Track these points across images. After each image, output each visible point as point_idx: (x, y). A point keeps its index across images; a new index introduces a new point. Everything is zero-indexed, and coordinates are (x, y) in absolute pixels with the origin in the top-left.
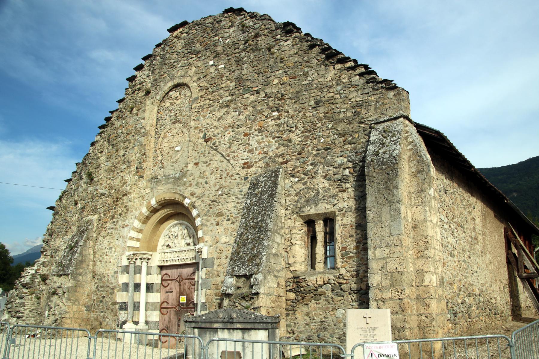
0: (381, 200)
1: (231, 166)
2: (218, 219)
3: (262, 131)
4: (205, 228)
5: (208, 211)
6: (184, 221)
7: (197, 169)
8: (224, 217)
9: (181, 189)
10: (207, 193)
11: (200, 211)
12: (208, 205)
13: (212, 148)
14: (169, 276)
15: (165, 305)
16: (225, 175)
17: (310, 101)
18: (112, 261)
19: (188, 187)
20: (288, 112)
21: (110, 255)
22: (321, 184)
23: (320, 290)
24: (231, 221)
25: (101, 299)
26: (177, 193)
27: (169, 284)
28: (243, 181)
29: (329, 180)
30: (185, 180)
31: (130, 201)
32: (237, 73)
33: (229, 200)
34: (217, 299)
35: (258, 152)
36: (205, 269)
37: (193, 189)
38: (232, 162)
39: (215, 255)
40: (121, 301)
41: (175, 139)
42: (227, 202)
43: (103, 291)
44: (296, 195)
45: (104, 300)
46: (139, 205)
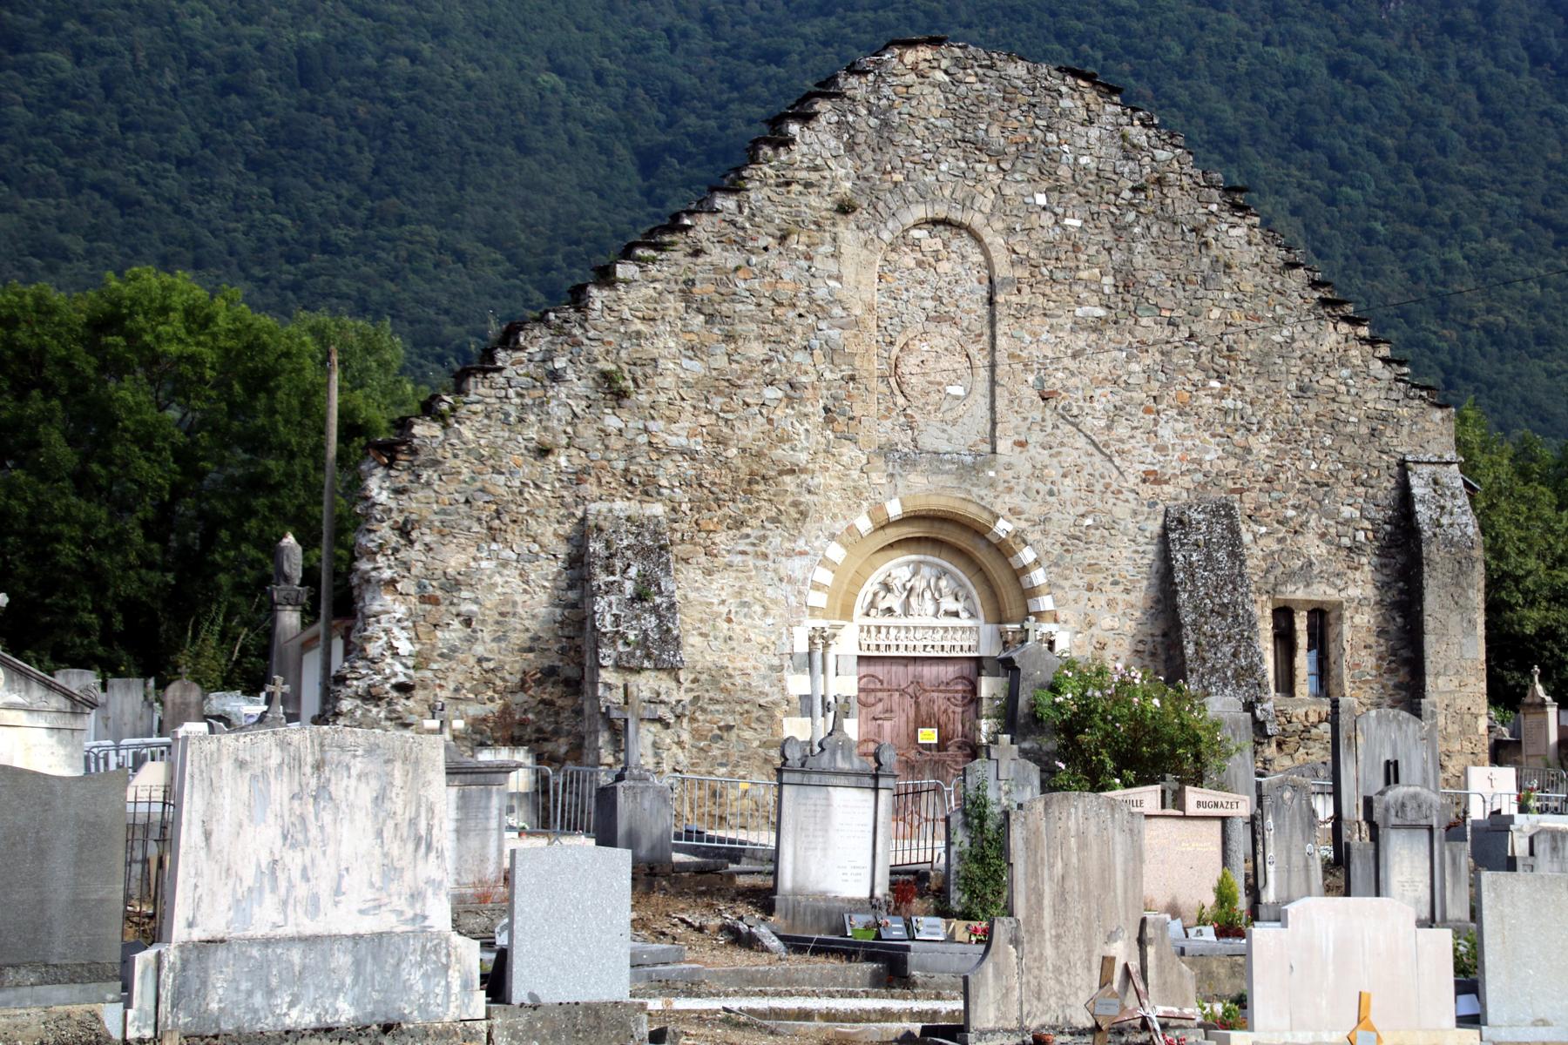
0: (1449, 602)
1: (1116, 473)
2: (1087, 578)
3: (1188, 414)
4: (1059, 593)
5: (1061, 557)
9: (983, 493)
10: (1056, 516)
11: (1042, 553)
14: (881, 682)
16: (1098, 487)
17: (1288, 382)
20: (1242, 389)
21: (748, 621)
22: (1313, 547)
23: (1314, 731)
24: (1121, 587)
28: (1146, 509)
29: (1330, 543)
30: (992, 474)
31: (809, 492)
32: (1117, 256)
35: (1177, 454)
37: (1016, 500)
38: (1117, 460)
41: (945, 363)
43: (724, 712)
44: (1264, 559)
45: (733, 735)
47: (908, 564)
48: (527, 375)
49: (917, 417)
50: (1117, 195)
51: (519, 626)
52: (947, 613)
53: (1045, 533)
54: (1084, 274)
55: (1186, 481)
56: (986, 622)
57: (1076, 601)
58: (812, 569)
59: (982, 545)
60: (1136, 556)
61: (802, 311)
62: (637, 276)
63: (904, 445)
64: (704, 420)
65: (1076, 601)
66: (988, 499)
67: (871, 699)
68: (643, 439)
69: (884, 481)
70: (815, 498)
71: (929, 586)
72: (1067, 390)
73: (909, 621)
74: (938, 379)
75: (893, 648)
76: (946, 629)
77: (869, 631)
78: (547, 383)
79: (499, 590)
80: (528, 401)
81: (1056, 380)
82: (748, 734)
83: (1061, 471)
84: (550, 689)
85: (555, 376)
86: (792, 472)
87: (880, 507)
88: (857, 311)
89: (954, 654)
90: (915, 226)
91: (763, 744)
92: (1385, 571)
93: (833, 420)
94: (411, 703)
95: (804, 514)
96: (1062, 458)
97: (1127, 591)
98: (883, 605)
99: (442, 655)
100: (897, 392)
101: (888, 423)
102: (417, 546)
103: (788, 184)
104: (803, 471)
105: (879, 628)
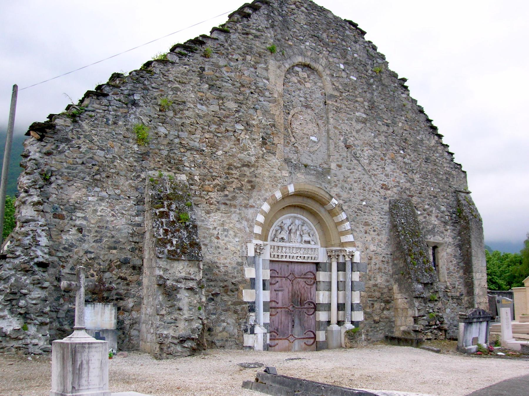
2: (366, 228)
4: (355, 234)
6: (303, 215)
8: (370, 227)
11: (348, 215)
14: (278, 273)
15: (273, 305)
18: (229, 247)
21: (227, 239)
24: (376, 233)
25: (212, 297)
27: (277, 282)
28: (383, 200)
30: (329, 178)
31: (256, 176)
33: (373, 213)
34: (370, 301)
36: (358, 272)
39: (366, 261)
42: (372, 214)
45: (218, 299)
48: (120, 101)
49: (299, 148)
50: (367, 72)
51: (109, 235)
54: (359, 99)
55: (395, 190)
56: (321, 247)
59: (322, 210)
60: (380, 219)
61: (253, 91)
62: (177, 61)
64: (207, 136)
66: (328, 189)
68: (177, 141)
69: (287, 175)
73: (291, 245)
78: (130, 106)
79: (99, 214)
80: (119, 114)
81: (350, 141)
82: (226, 298)
83: (354, 180)
84: (124, 271)
85: (134, 103)
86: (248, 166)
87: (286, 187)
88: (276, 96)
90: (297, 65)
91: (234, 304)
92: (454, 232)
94: (46, 275)
95: (253, 187)
97: (378, 235)
98: (280, 236)
99: (65, 248)
102: (53, 185)
103: (247, 34)
105: (278, 247)
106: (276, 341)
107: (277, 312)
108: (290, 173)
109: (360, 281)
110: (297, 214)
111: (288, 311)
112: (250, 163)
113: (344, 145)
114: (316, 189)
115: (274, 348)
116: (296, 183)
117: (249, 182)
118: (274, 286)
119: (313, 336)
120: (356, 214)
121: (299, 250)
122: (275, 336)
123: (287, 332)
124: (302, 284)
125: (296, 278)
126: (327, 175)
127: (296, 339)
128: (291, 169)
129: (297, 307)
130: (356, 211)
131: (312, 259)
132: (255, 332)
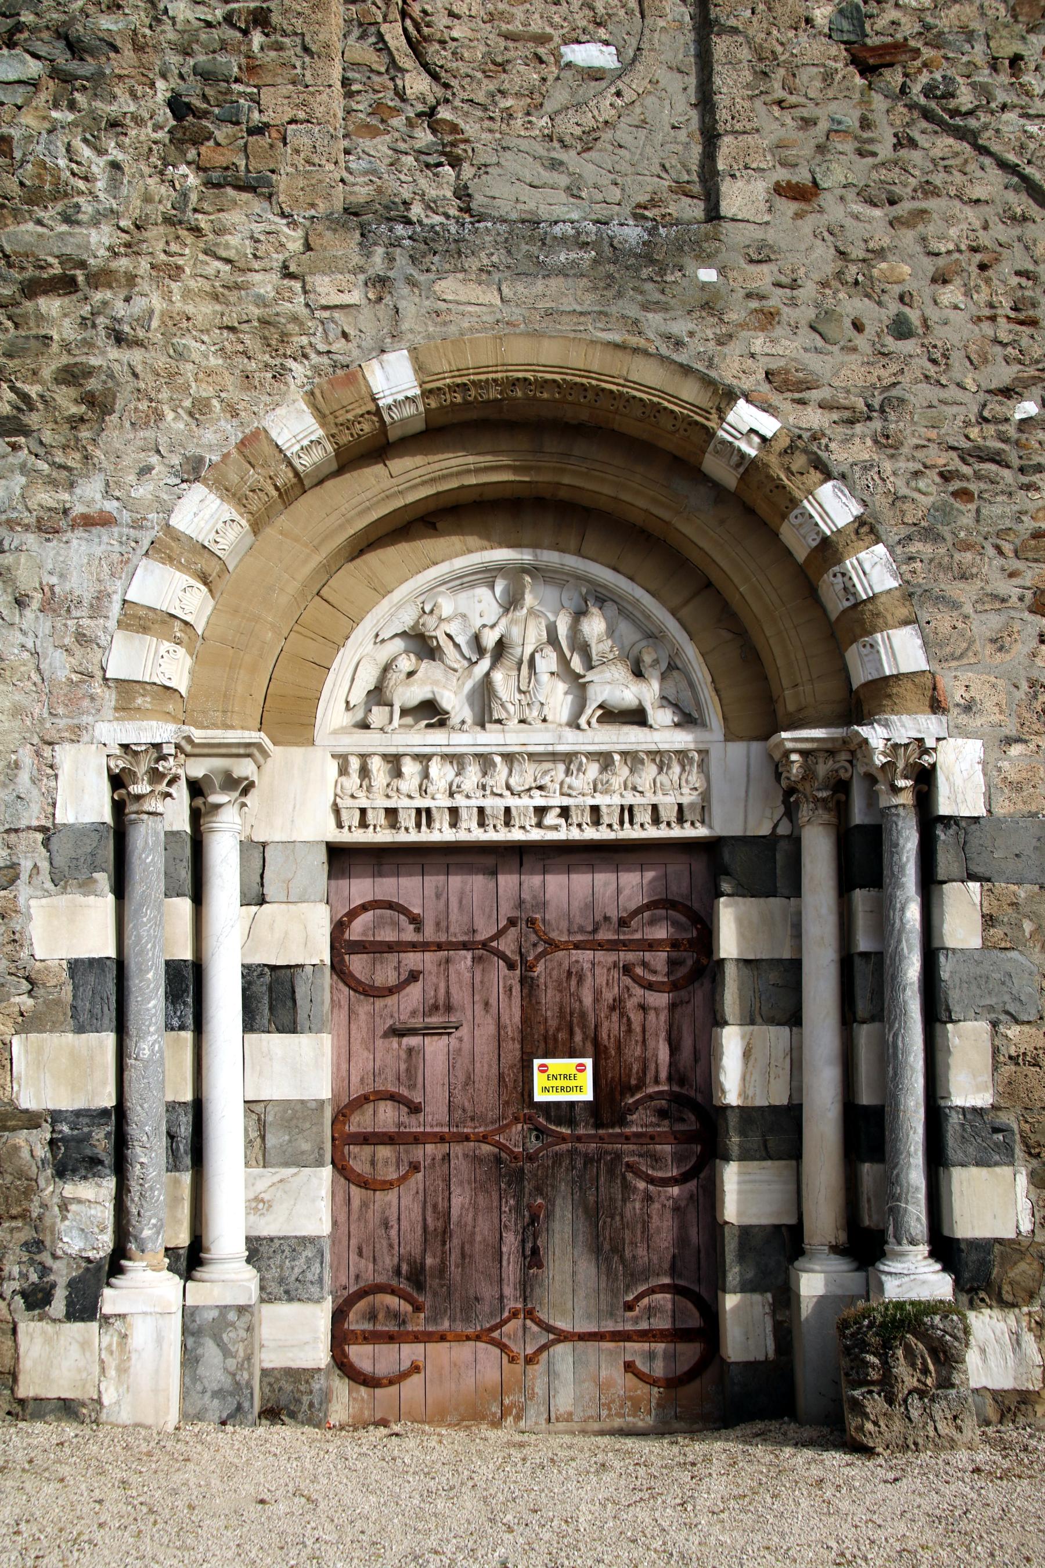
4: (943, 621)
5: (944, 511)
6: (579, 553)
7: (807, 225)
9: (680, 327)
10: (921, 394)
11: (881, 502)
12: (933, 475)
13: (927, 115)
14: (416, 921)
19: (743, 326)
26: (646, 353)
27: (414, 976)
30: (708, 275)
31: (119, 339)
36: (974, 886)
40: (66, 1103)
46: (229, 381)
47: (488, 575)
49: (470, 128)
52: (611, 715)
53: (886, 442)
56: (730, 736)
57: (998, 643)
58: (125, 569)
63: (430, 207)
65: (998, 643)
66: (695, 346)
67: (386, 974)
69: (355, 297)
70: (136, 356)
71: (553, 640)
72: (938, 42)
73: (490, 739)
74: (537, 26)
75: (442, 821)
76: (605, 760)
77: (365, 772)
83: (929, 266)
86: (65, 285)
89: (631, 833)
93: (199, 139)
96: (931, 230)
98: (413, 694)
100: (406, 61)
101: (380, 147)
104: (101, 278)
106: (406, 1348)
107: (415, 1167)
108: (381, 282)
109: (987, 946)
110: (535, 545)
111: (498, 1160)
112: (82, 265)
113: (837, 50)
114: (597, 361)
115: (393, 1389)
116: (429, 337)
117: (71, 376)
118: (392, 1000)
119: (694, 1320)
120: (956, 485)
121: (561, 767)
122: (394, 1315)
123: (488, 1292)
124: (601, 980)
125: (554, 946)
126: (688, 262)
127: (563, 1337)
128: (390, 259)
129: (565, 1130)
130: (956, 464)
131: (656, 820)
132: (107, 1309)
